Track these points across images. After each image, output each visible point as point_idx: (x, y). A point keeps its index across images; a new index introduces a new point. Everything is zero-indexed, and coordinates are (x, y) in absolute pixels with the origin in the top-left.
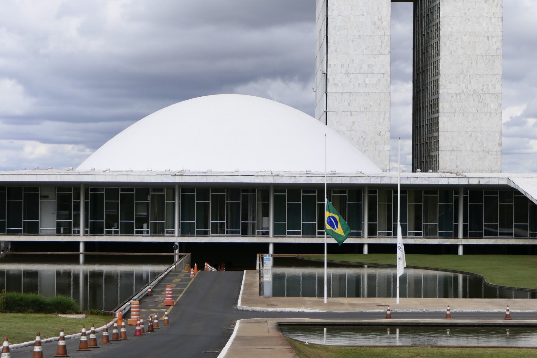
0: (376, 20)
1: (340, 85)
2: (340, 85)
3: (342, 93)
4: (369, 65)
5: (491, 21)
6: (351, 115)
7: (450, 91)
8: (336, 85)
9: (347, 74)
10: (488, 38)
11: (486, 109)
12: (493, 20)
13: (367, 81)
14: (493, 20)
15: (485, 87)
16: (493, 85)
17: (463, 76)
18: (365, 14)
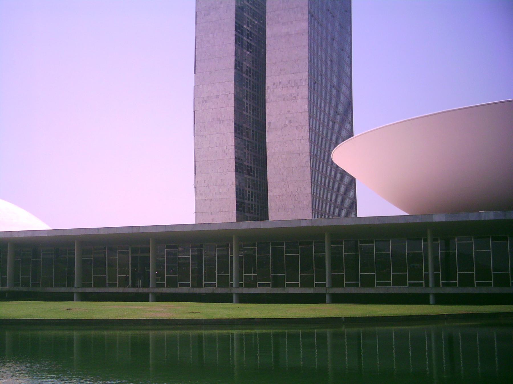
1: (204, 194)
2: (204, 194)
3: (205, 200)
6: (211, 214)
7: (275, 194)
8: (201, 194)
9: (208, 186)
10: (299, 154)
11: (300, 205)
13: (221, 190)
14: (302, 141)
15: (299, 189)
16: (304, 188)
17: (283, 183)
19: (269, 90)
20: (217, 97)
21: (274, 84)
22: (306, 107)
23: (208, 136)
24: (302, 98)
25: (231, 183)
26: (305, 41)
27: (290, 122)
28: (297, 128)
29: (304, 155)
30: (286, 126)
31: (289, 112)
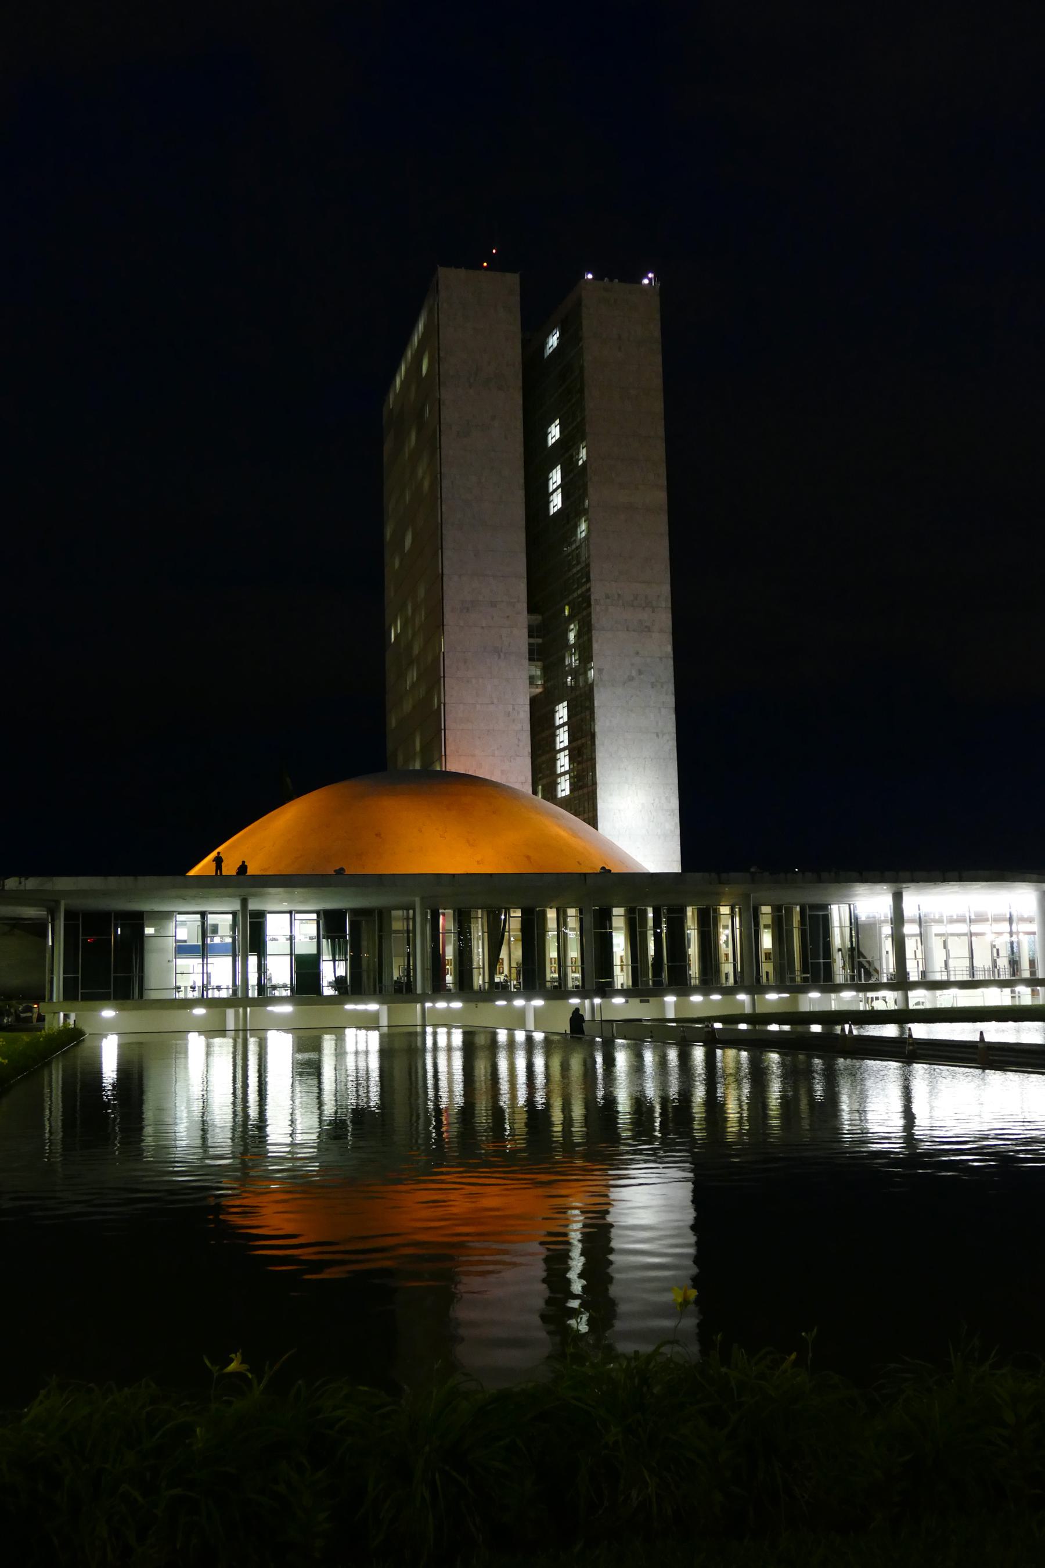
0: (510, 708)
4: (503, 772)
5: (660, 712)
12: (663, 710)
14: (663, 710)
18: (495, 701)
19: (598, 608)
20: (493, 604)
21: (607, 597)
22: (669, 649)
23: (474, 681)
24: (661, 631)
25: (522, 779)
26: (662, 524)
27: (640, 672)
28: (653, 685)
29: (666, 737)
30: (631, 679)
31: (637, 653)
